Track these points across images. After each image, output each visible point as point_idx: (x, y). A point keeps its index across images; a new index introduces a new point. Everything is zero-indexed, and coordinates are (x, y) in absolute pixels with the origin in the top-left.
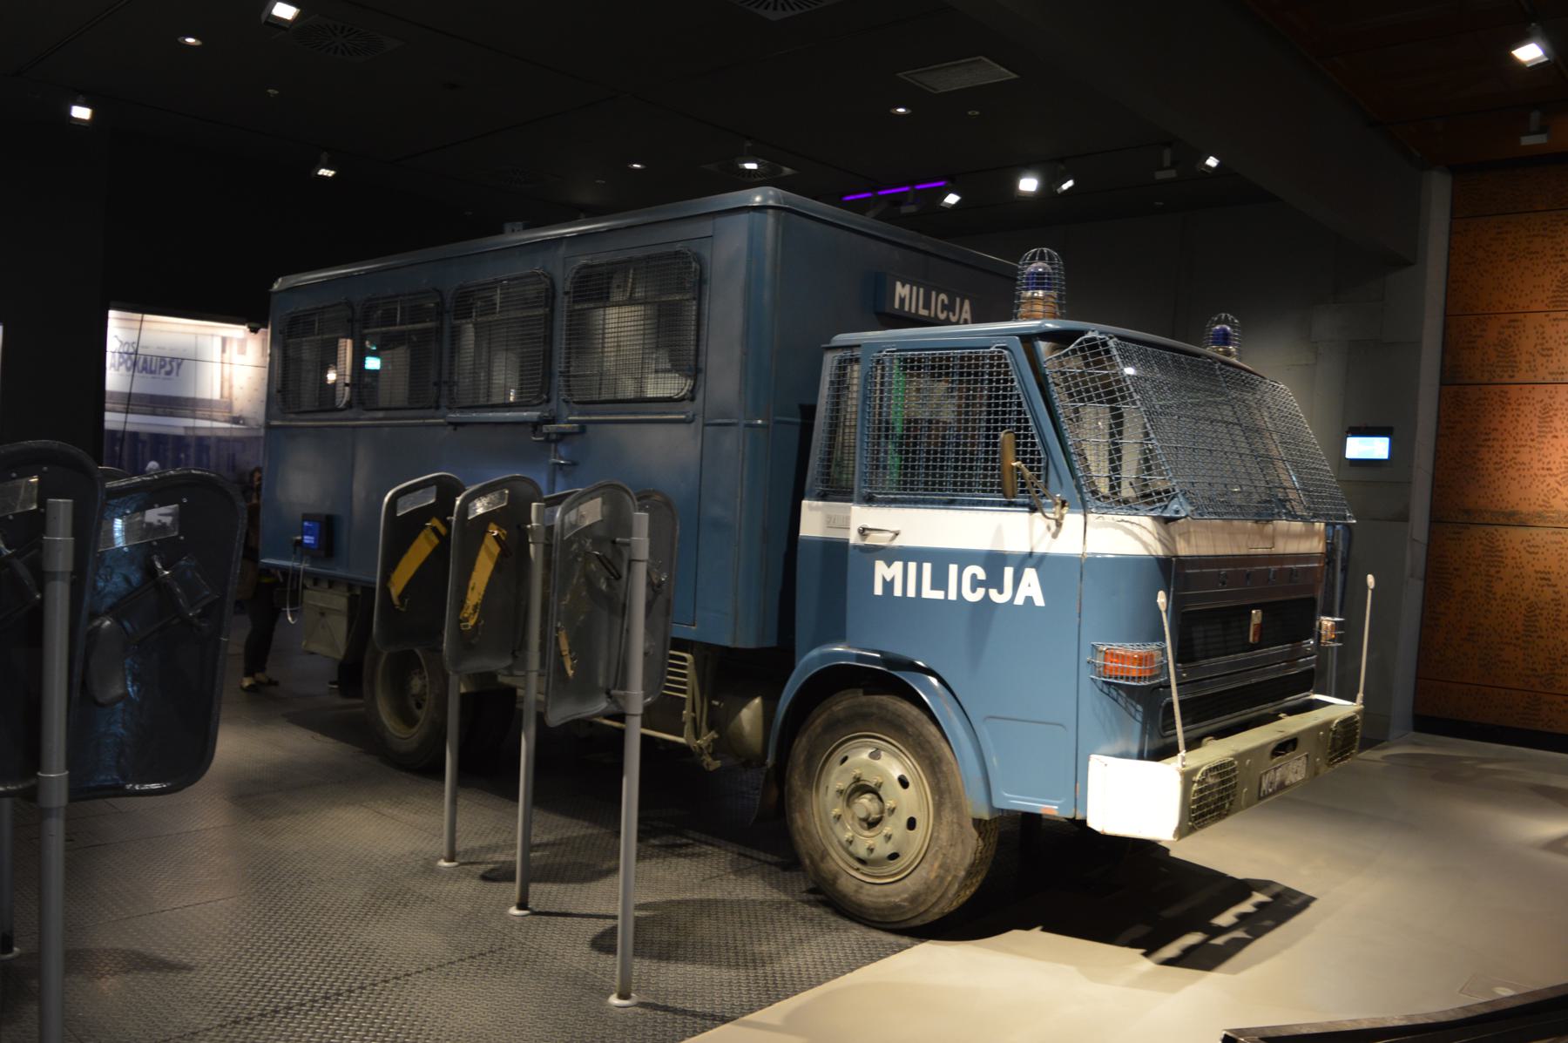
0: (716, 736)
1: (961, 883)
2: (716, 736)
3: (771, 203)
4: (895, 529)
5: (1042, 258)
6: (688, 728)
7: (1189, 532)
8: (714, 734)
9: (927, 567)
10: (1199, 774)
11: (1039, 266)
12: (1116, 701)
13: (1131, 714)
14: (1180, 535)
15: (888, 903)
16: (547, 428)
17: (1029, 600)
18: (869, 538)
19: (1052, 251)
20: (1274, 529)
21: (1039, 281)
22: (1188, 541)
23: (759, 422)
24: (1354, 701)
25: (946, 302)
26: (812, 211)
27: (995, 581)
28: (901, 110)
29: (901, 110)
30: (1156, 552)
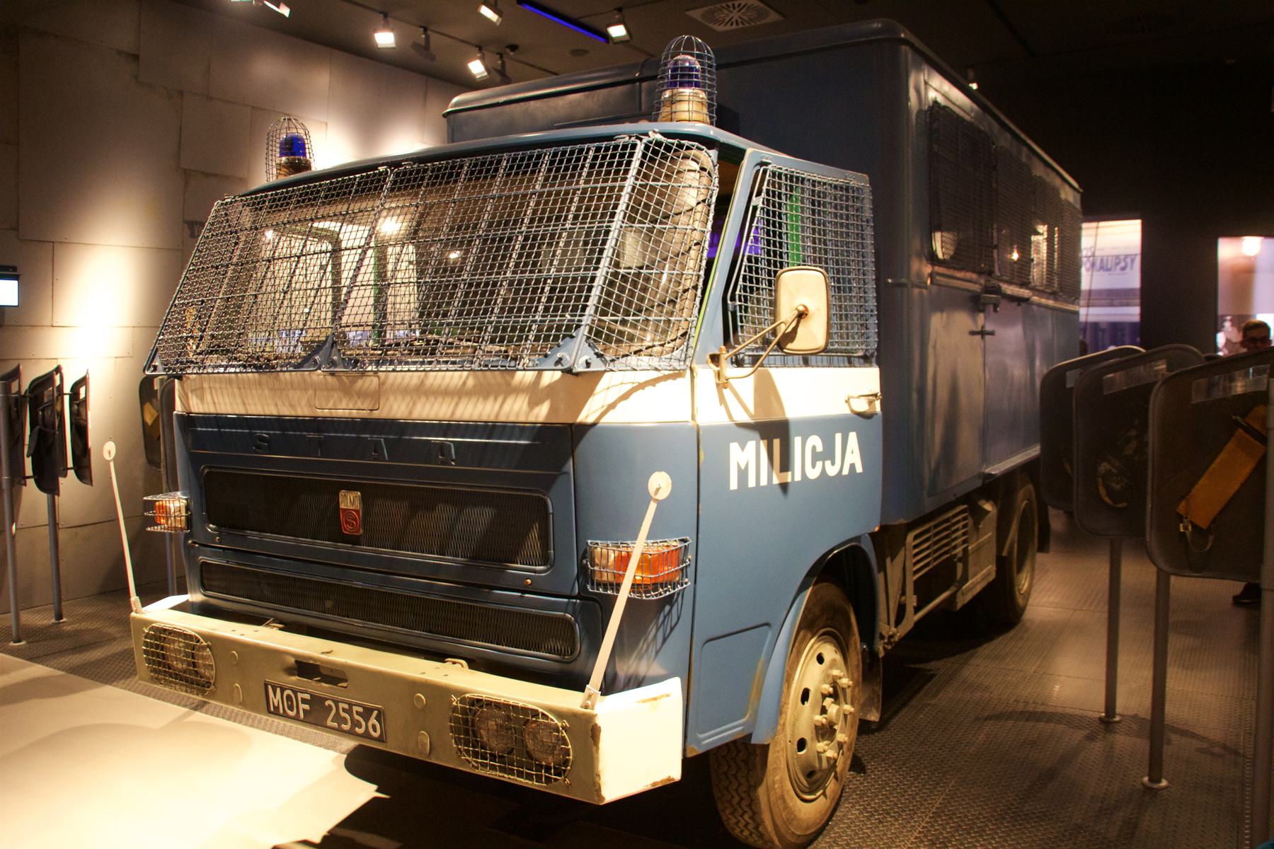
7: (202, 388)
14: (192, 391)
20: (381, 384)
22: (202, 399)
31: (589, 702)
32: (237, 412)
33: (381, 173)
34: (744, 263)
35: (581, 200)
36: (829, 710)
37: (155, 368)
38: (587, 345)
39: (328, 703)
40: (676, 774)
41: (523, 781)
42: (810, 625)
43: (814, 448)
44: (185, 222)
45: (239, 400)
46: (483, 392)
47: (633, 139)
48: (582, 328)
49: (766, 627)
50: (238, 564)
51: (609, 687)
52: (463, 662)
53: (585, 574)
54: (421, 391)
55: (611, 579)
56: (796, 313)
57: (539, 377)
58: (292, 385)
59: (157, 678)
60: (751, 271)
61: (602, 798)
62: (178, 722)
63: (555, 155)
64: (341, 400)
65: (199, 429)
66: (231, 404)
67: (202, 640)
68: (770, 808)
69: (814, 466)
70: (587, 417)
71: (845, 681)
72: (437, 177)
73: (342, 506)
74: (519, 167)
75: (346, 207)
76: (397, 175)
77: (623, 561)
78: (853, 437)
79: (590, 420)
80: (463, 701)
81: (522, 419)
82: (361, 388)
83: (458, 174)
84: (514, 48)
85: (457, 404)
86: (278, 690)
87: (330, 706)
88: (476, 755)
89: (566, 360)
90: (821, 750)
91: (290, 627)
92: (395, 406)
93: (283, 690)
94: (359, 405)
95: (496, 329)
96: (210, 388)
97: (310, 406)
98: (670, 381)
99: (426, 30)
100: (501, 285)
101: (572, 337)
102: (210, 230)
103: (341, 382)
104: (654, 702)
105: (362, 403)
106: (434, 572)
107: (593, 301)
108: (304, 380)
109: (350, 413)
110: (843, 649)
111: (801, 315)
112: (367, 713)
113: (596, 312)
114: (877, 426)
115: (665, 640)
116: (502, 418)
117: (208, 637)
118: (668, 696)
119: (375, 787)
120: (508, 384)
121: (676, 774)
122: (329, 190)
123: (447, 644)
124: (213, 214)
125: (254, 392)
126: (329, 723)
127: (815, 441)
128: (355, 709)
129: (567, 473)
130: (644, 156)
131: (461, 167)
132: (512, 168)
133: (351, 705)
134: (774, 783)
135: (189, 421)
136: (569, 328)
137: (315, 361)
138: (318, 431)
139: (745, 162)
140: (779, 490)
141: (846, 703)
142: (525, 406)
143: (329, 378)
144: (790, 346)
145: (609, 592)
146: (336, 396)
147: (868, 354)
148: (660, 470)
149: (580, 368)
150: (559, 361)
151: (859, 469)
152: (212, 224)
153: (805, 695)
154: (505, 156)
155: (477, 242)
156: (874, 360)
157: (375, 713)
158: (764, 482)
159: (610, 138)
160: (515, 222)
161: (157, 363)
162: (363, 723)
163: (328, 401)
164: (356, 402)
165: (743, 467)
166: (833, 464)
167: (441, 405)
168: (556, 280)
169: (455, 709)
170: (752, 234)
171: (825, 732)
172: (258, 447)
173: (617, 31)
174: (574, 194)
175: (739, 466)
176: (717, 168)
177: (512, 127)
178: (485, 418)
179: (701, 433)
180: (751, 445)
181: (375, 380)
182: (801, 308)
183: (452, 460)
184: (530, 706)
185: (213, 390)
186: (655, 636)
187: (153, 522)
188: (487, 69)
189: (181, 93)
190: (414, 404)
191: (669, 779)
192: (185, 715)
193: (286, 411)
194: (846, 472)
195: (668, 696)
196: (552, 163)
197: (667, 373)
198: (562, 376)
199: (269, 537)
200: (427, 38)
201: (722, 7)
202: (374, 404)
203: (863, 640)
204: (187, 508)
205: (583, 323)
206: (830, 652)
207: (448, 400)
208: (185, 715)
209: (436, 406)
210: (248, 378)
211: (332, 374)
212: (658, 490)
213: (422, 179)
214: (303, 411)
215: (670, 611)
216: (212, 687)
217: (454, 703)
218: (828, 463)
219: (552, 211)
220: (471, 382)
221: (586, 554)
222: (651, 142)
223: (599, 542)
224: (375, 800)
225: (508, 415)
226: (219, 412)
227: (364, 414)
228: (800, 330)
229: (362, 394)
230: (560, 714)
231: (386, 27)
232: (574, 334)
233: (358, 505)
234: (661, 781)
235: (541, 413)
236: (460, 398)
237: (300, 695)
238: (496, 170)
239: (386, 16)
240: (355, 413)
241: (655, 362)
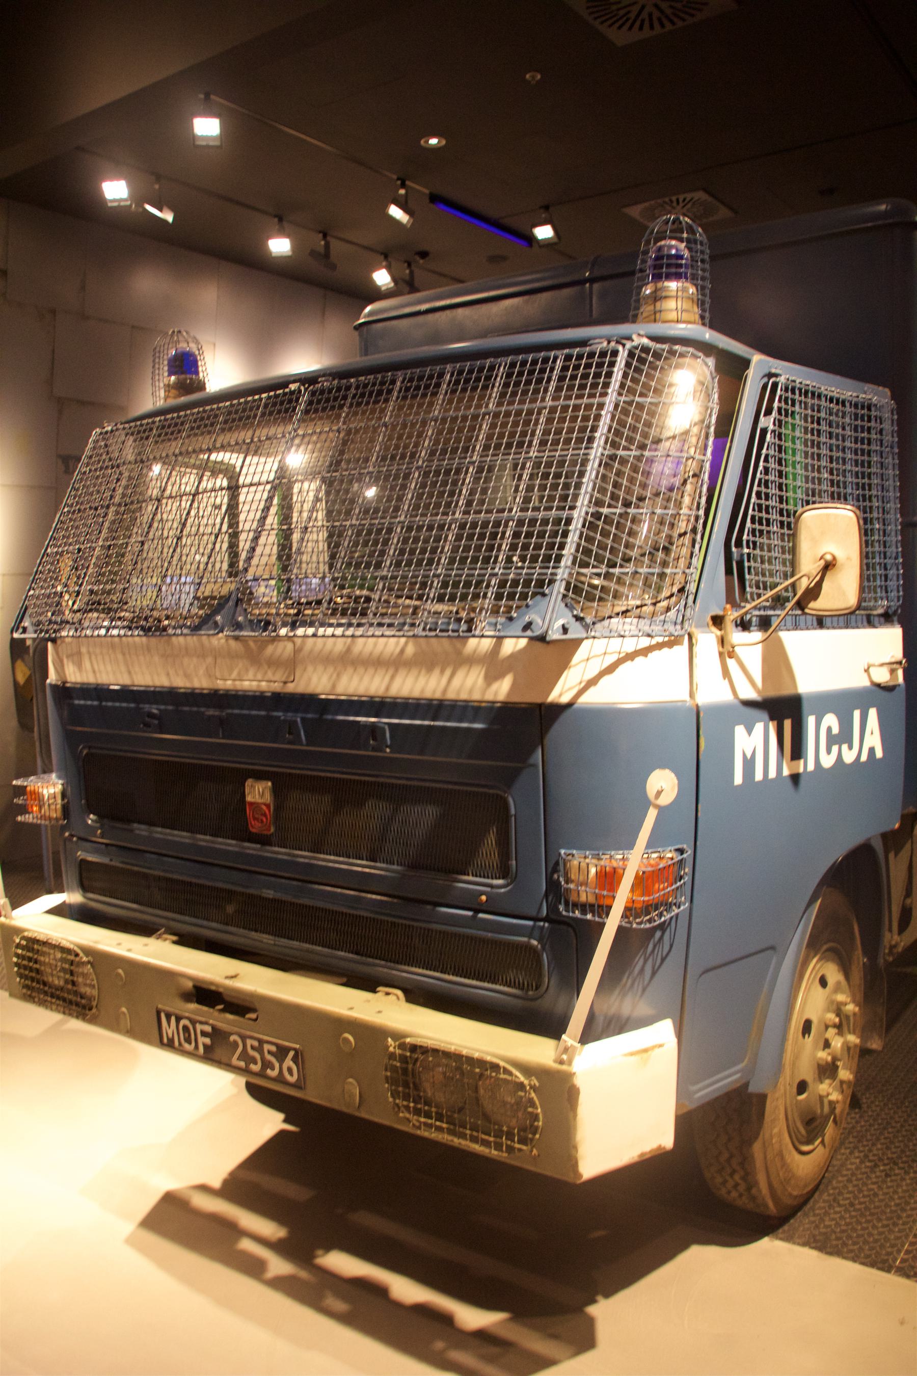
7: (79, 653)
14: (68, 657)
20: (297, 651)
22: (79, 665)
31: (565, 1057)
32: (121, 682)
33: (292, 393)
34: (753, 500)
35: (549, 421)
36: (833, 1044)
37: (25, 630)
38: (563, 605)
39: (232, 1038)
40: (668, 1141)
41: (477, 1148)
42: (814, 944)
43: (829, 729)
44: (59, 456)
45: (123, 668)
47: (613, 344)
48: (557, 583)
49: (769, 952)
50: (123, 862)
51: (588, 1036)
52: (399, 993)
53: (555, 891)
55: (592, 899)
56: (822, 563)
58: (187, 652)
59: (30, 996)
60: (760, 511)
61: (581, 1176)
62: (53, 1030)
63: (513, 365)
64: (247, 670)
65: (77, 702)
66: (114, 673)
67: (81, 954)
68: (766, 1164)
69: (829, 751)
70: (560, 695)
71: (851, 1008)
72: (363, 395)
73: (249, 798)
74: (467, 381)
75: (250, 433)
76: (313, 393)
77: (610, 879)
78: (873, 713)
79: (565, 699)
80: (402, 1046)
81: (476, 696)
82: (271, 655)
83: (390, 392)
84: (424, 255)
85: (393, 678)
86: (173, 1019)
87: (236, 1043)
88: (417, 1112)
89: (537, 624)
90: (824, 1093)
91: (186, 940)
92: (315, 679)
93: (178, 1019)
94: (270, 675)
95: (445, 585)
96: (89, 653)
97: (210, 676)
98: (666, 650)
99: (325, 236)
100: (449, 529)
101: (544, 595)
102: (88, 464)
103: (246, 646)
104: (645, 1055)
105: (274, 674)
106: (362, 882)
107: (569, 551)
108: (202, 645)
109: (259, 686)
110: (846, 970)
111: (828, 566)
112: (281, 1053)
113: (574, 563)
114: (899, 700)
115: (654, 973)
116: (451, 695)
118: (661, 1046)
119: (280, 1116)
120: (459, 653)
121: (668, 1141)
122: (230, 413)
123: (381, 968)
124: (90, 445)
125: (142, 658)
126: (235, 1061)
127: (831, 721)
128: (266, 1047)
129: (535, 766)
130: (628, 365)
131: (393, 382)
132: (457, 382)
133: (261, 1042)
134: (771, 1137)
135: (64, 692)
136: (540, 583)
137: (216, 623)
138: (220, 707)
139: (751, 372)
140: (789, 783)
141: (850, 1033)
142: (481, 681)
143: (232, 643)
144: (812, 605)
145: (589, 917)
146: (241, 665)
147: (890, 612)
148: (662, 767)
149: (555, 634)
150: (528, 626)
151: (879, 754)
152: (91, 457)
153: (807, 1027)
154: (449, 367)
155: (416, 475)
156: (895, 618)
157: (292, 1053)
158: (772, 774)
159: (584, 343)
160: (466, 450)
161: (26, 623)
162: (277, 1065)
163: (231, 671)
164: (266, 673)
165: (749, 756)
166: (850, 748)
167: (373, 676)
168: (520, 523)
169: (392, 1056)
170: (761, 464)
171: (827, 1070)
172: (147, 725)
173: (544, 232)
174: (539, 413)
175: (744, 755)
176: (716, 380)
177: (436, 338)
178: (428, 694)
179: (701, 715)
180: (759, 727)
181: (290, 646)
182: (829, 557)
183: (387, 747)
184: (489, 1058)
185: (93, 657)
186: (642, 970)
187: (24, 810)
188: (394, 279)
189: (53, 312)
190: (339, 676)
191: (660, 1147)
192: (60, 1023)
193: (180, 682)
194: (864, 758)
195: (661, 1046)
196: (509, 376)
197: (660, 639)
198: (528, 643)
199: (159, 832)
200: (327, 246)
201: (665, 202)
202: (288, 676)
203: (865, 953)
204: (64, 795)
205: (558, 577)
206: (833, 974)
207: (381, 672)
208: (60, 1023)
209: (366, 679)
211: (237, 638)
212: (659, 793)
213: (345, 398)
214: (200, 681)
215: (661, 938)
216: (94, 1010)
217: (391, 1049)
218: (845, 747)
219: (512, 435)
220: (410, 650)
221: (555, 866)
222: (636, 348)
223: (574, 852)
224: (281, 1134)
225: (458, 692)
226: (100, 681)
227: (277, 687)
228: (826, 585)
229: (274, 663)
230: (527, 1070)
231: (282, 233)
232: (547, 591)
233: (268, 798)
234: (650, 1151)
236: (396, 670)
237: (199, 1027)
238: (438, 385)
239: (281, 219)
240: (264, 686)
241: (644, 625)
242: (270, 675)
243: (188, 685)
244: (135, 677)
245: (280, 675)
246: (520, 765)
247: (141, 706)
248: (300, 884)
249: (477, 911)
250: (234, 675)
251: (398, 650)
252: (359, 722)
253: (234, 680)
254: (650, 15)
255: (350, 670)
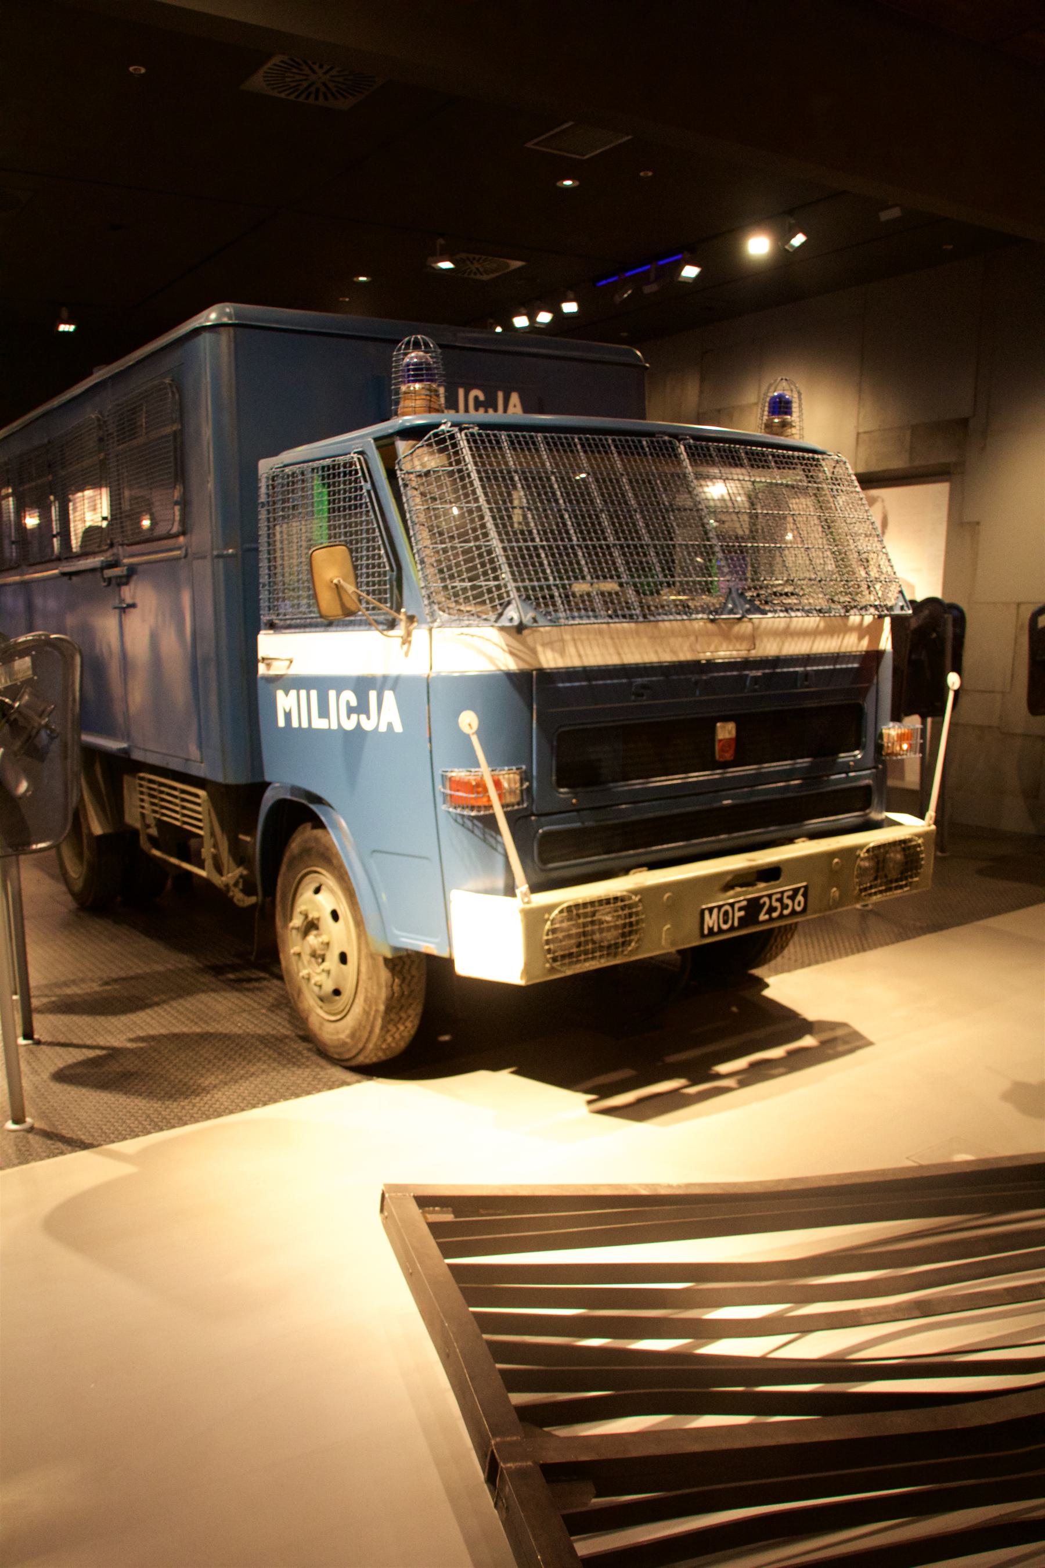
0: (245, 872)
1: (383, 1019)
2: (245, 872)
3: (225, 320)
4: (289, 657)
5: (417, 345)
6: (209, 862)
8: (241, 871)
9: (314, 693)
10: (556, 912)
11: (414, 356)
12: (473, 832)
13: (492, 847)
14: (544, 645)
15: (338, 1040)
16: (109, 573)
17: (390, 725)
18: (272, 667)
19: (427, 339)
21: (419, 373)
23: (230, 551)
24: (922, 816)
25: (482, 397)
26: (277, 322)
27: (362, 708)
28: (568, 183)
29: (568, 183)
30: (506, 666)
39: (762, 901)
45: (612, 650)
46: (830, 631)
54: (787, 633)
57: (862, 619)
58: (673, 633)
64: (721, 644)
65: (561, 685)
66: (602, 655)
81: (854, 649)
85: (813, 642)
91: (653, 866)
92: (768, 647)
96: (574, 640)
103: (720, 628)
108: (686, 628)
116: (843, 650)
117: (635, 892)
120: (846, 625)
123: (789, 830)
125: (631, 641)
133: (782, 893)
142: (856, 641)
143: (710, 626)
157: (802, 890)
163: (709, 645)
178: (832, 650)
181: (750, 625)
207: (807, 639)
209: (799, 645)
210: (623, 627)
211: (712, 621)
214: (685, 655)
220: (822, 625)
229: (740, 638)
235: (864, 645)
242: (738, 647)
243: (675, 659)
244: (623, 656)
245: (745, 646)
246: (867, 685)
247: (633, 680)
248: (749, 789)
249: (847, 773)
250: (712, 648)
251: (815, 625)
252: (797, 672)
253: (712, 652)
254: (318, 90)
255: (789, 639)
